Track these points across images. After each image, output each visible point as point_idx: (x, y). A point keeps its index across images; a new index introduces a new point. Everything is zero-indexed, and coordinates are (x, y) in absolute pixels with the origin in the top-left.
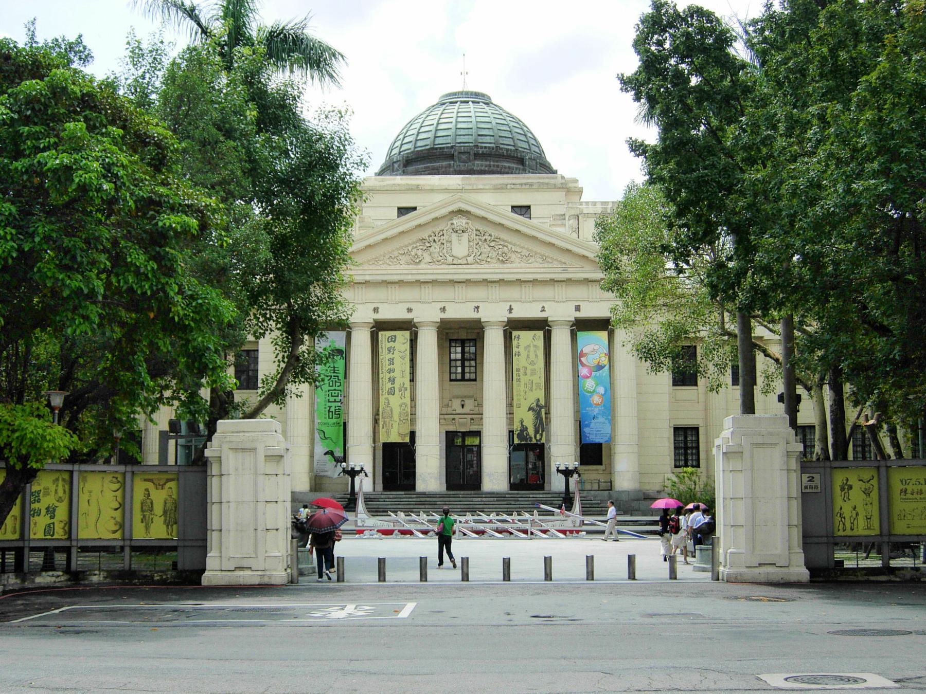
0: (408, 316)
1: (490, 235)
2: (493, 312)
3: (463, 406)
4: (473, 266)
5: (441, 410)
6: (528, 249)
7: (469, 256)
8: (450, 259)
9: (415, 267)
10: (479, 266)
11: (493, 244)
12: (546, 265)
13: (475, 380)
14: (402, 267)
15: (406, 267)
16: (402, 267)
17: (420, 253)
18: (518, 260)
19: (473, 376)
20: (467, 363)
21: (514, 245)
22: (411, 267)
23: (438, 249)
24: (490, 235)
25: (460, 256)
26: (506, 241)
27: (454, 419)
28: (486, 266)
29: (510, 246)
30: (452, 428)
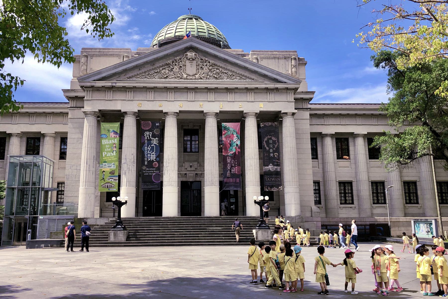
0: (160, 109)
1: (209, 62)
2: (211, 106)
3: (191, 166)
4: (200, 80)
5: (178, 169)
6: (231, 71)
7: (196, 74)
8: (185, 76)
9: (164, 80)
10: (202, 80)
11: (210, 68)
12: (242, 80)
13: (198, 152)
14: (156, 80)
15: (159, 80)
16: (156, 80)
17: (167, 71)
18: (225, 78)
19: (197, 150)
20: (193, 143)
21: (224, 68)
22: (162, 80)
23: (178, 70)
24: (209, 62)
25: (191, 74)
26: (219, 66)
27: (186, 174)
28: (207, 80)
29: (221, 69)
30: (184, 179)
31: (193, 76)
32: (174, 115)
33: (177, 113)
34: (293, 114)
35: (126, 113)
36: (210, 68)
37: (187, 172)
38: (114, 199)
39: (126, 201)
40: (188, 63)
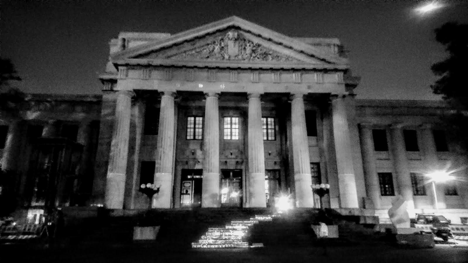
7: (239, 55)
30: (224, 167)
31: (236, 56)
32: (215, 96)
33: (218, 94)
34: (344, 96)
35: (163, 93)
36: (254, 48)
37: (228, 161)
38: (143, 186)
39: (158, 189)
40: (231, 44)
